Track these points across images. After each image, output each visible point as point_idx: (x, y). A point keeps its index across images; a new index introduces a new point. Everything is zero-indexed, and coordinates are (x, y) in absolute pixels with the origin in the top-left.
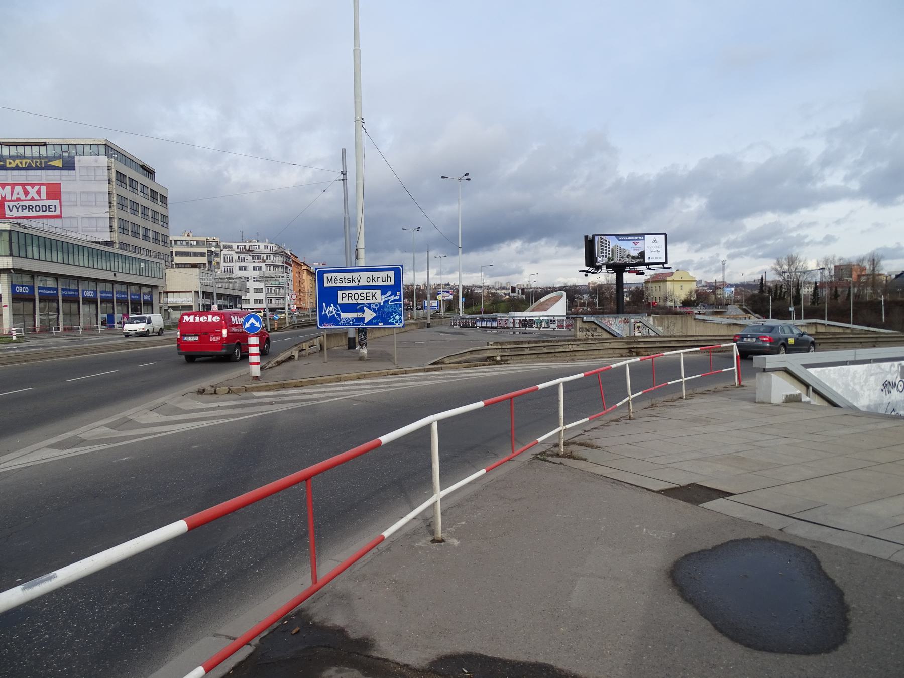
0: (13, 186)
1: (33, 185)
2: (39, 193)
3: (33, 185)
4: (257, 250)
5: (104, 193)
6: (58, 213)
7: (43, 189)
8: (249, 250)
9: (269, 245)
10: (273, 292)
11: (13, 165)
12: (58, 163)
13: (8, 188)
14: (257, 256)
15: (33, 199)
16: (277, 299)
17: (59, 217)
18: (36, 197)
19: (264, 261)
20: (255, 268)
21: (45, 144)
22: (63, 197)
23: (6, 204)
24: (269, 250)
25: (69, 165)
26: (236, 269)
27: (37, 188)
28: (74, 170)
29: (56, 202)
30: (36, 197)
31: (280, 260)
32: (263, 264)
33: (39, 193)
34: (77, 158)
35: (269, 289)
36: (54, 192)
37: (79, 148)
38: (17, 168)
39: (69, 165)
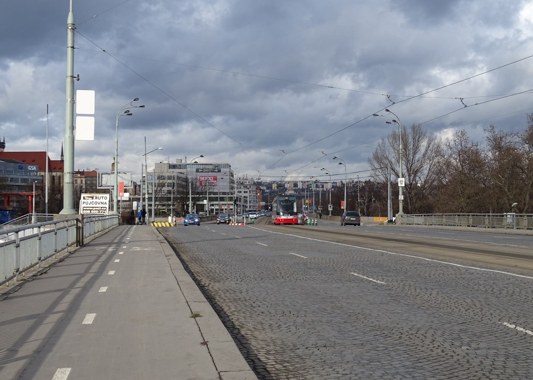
0: (205, 177)
1: (210, 177)
2: (211, 178)
3: (210, 177)
4: (245, 184)
5: (228, 179)
6: (216, 184)
7: (213, 177)
8: (242, 184)
9: (250, 181)
10: (252, 203)
11: (205, 171)
12: (217, 171)
13: (204, 177)
14: (246, 187)
15: (210, 180)
16: (253, 206)
17: (216, 185)
18: (211, 180)
19: (248, 189)
20: (244, 192)
21: (212, 164)
22: (218, 180)
23: (203, 182)
24: (250, 184)
25: (219, 171)
26: (236, 192)
27: (211, 177)
28: (220, 172)
29: (216, 181)
30: (211, 180)
31: (254, 188)
32: (248, 190)
33: (211, 178)
34: (221, 169)
35: (250, 202)
36: (215, 179)
37: (221, 165)
38: (206, 172)
39: (219, 171)
